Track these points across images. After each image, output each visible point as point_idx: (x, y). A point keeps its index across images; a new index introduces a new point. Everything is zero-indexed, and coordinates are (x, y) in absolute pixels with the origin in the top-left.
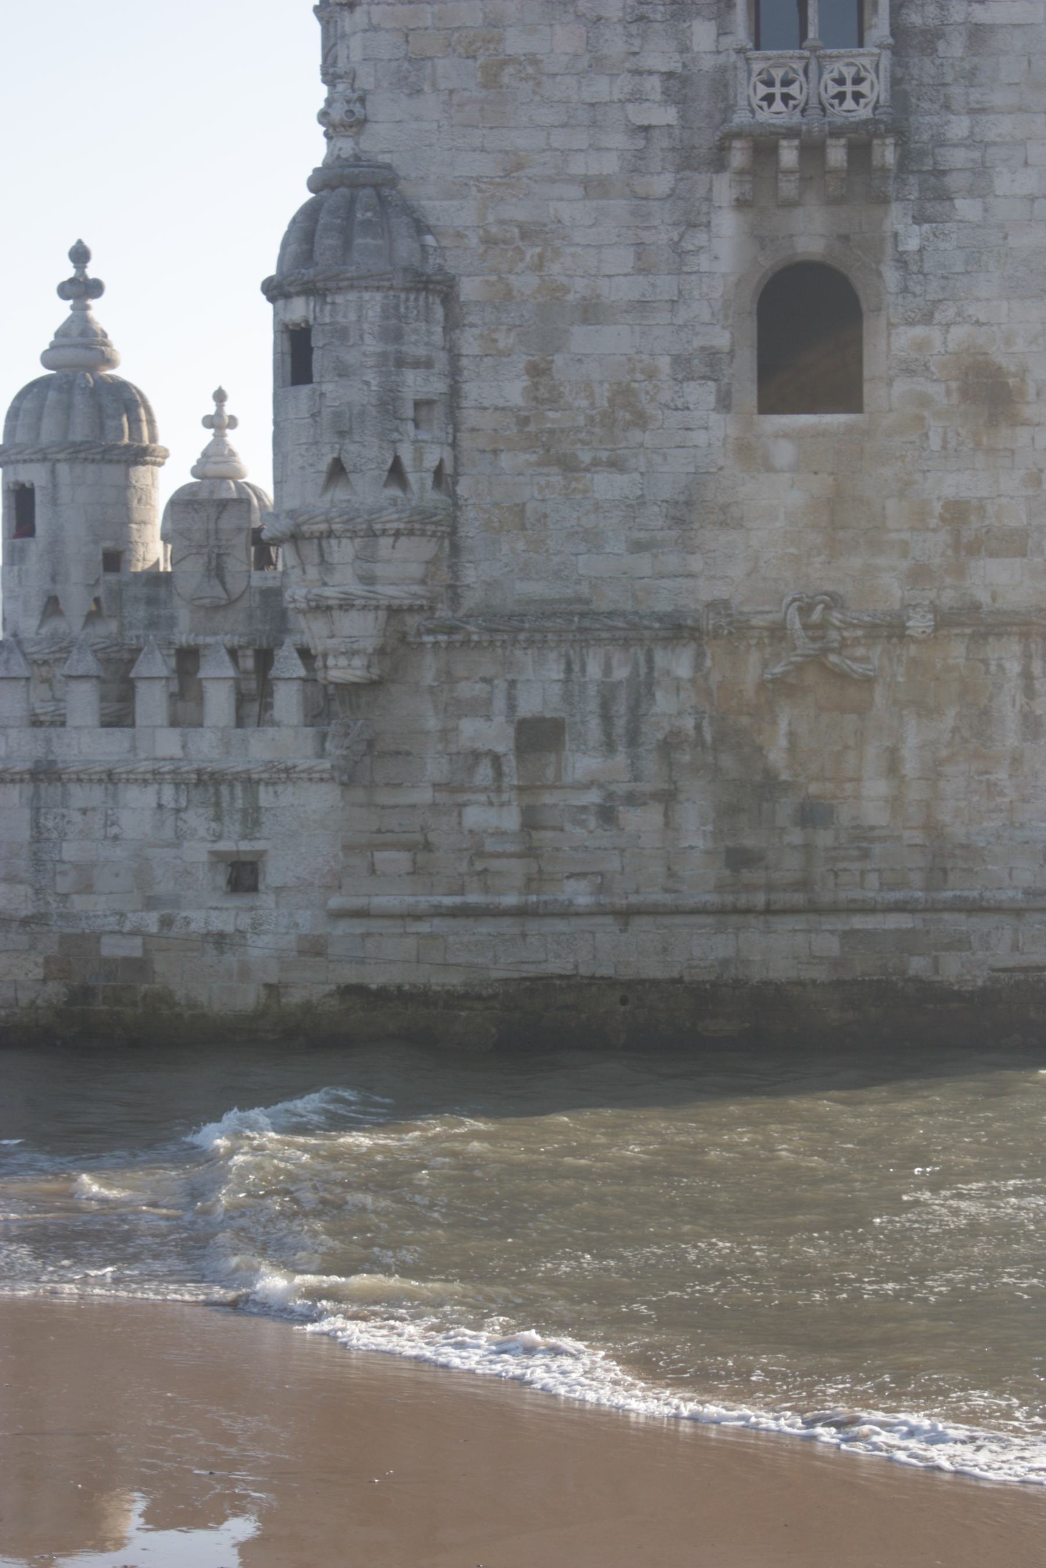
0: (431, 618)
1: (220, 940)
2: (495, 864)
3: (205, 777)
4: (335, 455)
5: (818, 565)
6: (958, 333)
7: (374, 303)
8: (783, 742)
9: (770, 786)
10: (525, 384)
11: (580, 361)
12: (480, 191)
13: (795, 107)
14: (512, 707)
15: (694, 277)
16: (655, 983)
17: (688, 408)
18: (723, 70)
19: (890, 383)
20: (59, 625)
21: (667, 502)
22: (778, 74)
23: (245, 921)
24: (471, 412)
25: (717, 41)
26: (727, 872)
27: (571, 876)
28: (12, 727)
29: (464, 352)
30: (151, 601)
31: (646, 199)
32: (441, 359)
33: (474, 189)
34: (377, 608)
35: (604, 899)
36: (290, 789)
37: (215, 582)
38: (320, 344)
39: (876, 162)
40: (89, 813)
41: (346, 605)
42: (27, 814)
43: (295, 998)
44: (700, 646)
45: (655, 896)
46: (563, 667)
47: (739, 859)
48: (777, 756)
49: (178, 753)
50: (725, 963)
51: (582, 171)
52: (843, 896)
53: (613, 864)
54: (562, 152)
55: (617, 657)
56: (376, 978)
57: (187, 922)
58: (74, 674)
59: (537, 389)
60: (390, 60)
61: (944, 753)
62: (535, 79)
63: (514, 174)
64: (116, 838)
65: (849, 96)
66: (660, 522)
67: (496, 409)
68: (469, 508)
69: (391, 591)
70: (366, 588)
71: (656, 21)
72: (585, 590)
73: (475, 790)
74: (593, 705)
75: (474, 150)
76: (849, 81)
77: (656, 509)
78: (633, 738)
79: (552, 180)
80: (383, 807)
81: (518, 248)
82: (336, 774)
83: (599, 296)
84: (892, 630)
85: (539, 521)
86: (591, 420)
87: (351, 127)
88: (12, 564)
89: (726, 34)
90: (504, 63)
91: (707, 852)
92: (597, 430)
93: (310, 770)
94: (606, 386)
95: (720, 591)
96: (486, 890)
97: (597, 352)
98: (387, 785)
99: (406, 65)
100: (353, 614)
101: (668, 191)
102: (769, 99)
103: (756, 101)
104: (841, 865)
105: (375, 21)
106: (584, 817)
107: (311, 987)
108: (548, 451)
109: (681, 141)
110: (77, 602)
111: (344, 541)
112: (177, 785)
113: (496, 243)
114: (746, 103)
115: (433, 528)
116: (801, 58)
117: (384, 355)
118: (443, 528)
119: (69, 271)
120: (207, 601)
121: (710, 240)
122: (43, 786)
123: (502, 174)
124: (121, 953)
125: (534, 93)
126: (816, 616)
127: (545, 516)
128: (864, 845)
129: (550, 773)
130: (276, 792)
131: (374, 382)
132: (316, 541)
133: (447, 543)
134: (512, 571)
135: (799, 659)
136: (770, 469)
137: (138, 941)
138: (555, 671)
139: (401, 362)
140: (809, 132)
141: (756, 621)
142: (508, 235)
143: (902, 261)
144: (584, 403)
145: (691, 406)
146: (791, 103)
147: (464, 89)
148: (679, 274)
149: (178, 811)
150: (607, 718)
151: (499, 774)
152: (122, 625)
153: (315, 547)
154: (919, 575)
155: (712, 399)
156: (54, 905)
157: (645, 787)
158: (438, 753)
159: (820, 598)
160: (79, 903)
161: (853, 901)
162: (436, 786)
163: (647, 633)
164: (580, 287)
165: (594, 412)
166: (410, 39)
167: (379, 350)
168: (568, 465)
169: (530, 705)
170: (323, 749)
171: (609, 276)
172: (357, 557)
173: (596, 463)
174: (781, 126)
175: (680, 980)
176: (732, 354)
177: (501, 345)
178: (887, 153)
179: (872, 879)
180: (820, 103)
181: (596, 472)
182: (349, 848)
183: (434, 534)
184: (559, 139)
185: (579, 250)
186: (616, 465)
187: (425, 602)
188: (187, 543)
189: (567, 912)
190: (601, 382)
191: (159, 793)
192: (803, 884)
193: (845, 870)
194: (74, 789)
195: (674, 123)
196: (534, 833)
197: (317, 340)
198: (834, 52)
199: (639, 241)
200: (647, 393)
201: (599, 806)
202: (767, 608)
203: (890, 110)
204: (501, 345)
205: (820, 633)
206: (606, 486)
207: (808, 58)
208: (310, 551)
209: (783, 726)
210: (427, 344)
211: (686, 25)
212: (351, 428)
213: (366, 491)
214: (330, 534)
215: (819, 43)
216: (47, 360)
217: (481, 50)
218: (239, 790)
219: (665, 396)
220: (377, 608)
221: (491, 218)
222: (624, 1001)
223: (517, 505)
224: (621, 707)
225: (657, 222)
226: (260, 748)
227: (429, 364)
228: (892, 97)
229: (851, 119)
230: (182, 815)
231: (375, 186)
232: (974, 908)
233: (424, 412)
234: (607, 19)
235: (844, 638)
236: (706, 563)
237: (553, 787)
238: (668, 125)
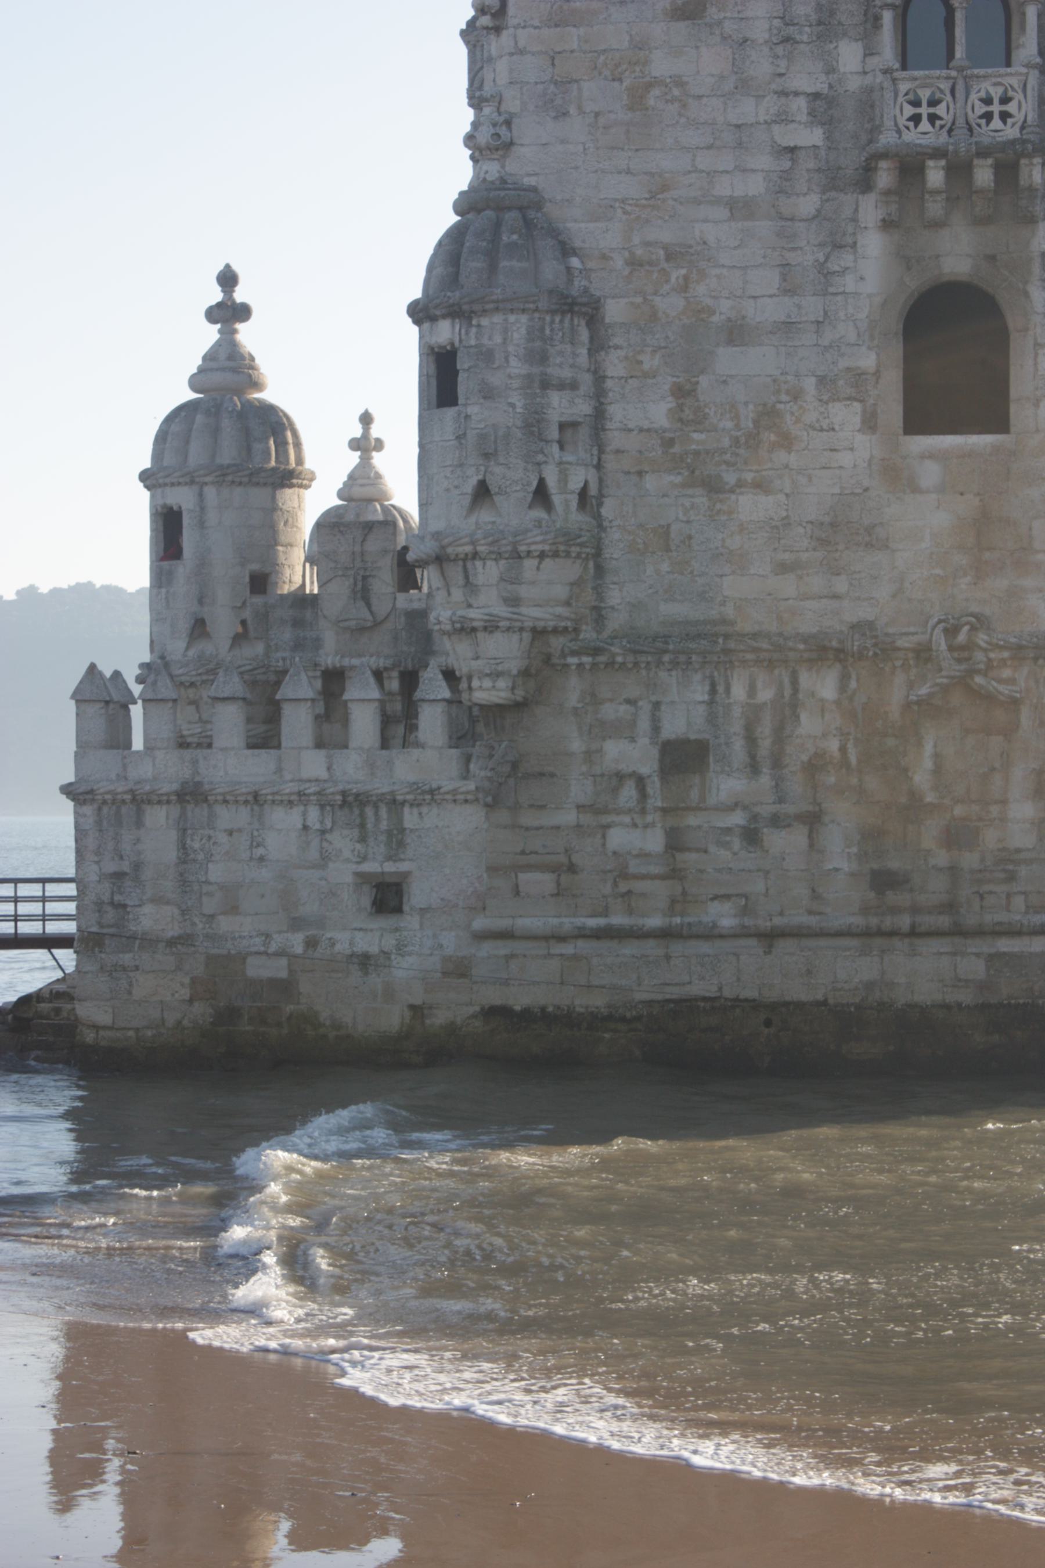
0: (575, 640)
1: (364, 961)
2: (639, 886)
3: (350, 799)
4: (480, 477)
5: (963, 586)
7: (519, 325)
8: (928, 764)
10: (670, 405)
11: (725, 382)
12: (625, 213)
13: (942, 127)
14: (656, 729)
15: (839, 298)
16: (799, 1005)
17: (833, 429)
18: (869, 90)
20: (207, 647)
21: (812, 523)
22: (925, 95)
23: (389, 942)
24: (616, 433)
25: (864, 62)
26: (872, 895)
27: (715, 898)
28: (159, 749)
29: (609, 373)
30: (298, 623)
31: (792, 219)
32: (586, 380)
33: (619, 211)
34: (521, 629)
35: (748, 921)
36: (435, 810)
37: (361, 604)
38: (466, 366)
39: (1023, 182)
41: (491, 627)
42: (173, 835)
43: (439, 1019)
44: (845, 667)
45: (800, 918)
46: (707, 688)
47: (884, 881)
48: (921, 778)
49: (323, 774)
50: (870, 986)
51: (728, 193)
52: (988, 918)
53: (760, 886)
54: (708, 174)
56: (520, 999)
57: (332, 943)
58: (221, 695)
59: (682, 411)
60: (536, 83)
62: (681, 101)
63: (659, 196)
64: (262, 859)
65: (996, 116)
67: (641, 430)
68: (614, 529)
69: (536, 612)
70: (511, 609)
71: (802, 42)
72: (729, 611)
73: (618, 812)
74: (737, 727)
75: (620, 173)
76: (996, 101)
77: (801, 530)
79: (697, 202)
80: (527, 829)
81: (663, 269)
82: (480, 796)
83: (744, 318)
85: (683, 542)
86: (736, 441)
87: (497, 150)
88: (160, 587)
89: (872, 54)
90: (649, 86)
91: (852, 874)
92: (742, 451)
93: (454, 792)
94: (751, 407)
95: (864, 612)
96: (630, 912)
97: (742, 372)
98: (531, 806)
99: (552, 87)
100: (498, 635)
101: (813, 212)
102: (916, 119)
103: (902, 121)
104: (986, 888)
105: (521, 44)
106: (728, 838)
107: (455, 1008)
108: (693, 472)
109: (827, 162)
110: (223, 623)
111: (489, 563)
112: (322, 807)
113: (641, 265)
114: (893, 123)
115: (578, 549)
116: (948, 78)
117: (529, 377)
118: (588, 550)
119: (216, 295)
120: (353, 623)
121: (855, 261)
122: (190, 807)
123: (647, 196)
124: (266, 973)
125: (680, 115)
126: (962, 637)
127: (690, 537)
128: (1011, 867)
129: (694, 794)
130: (420, 814)
131: (519, 404)
132: (461, 563)
133: (591, 564)
134: (657, 592)
135: (945, 681)
136: (916, 489)
137: (284, 962)
138: (699, 693)
139: (546, 384)
140: (956, 152)
141: (900, 643)
142: (654, 257)
144: (729, 425)
145: (837, 427)
146: (938, 123)
147: (610, 112)
148: (824, 295)
149: (323, 832)
150: (751, 740)
151: (643, 795)
153: (460, 569)
155: (857, 420)
157: (790, 809)
158: (583, 774)
159: (965, 619)
160: (225, 924)
161: (1000, 923)
162: (580, 808)
164: (725, 307)
165: (739, 434)
166: (556, 62)
167: (524, 372)
168: (713, 487)
169: (674, 726)
170: (468, 771)
171: (754, 297)
172: (502, 579)
173: (740, 484)
174: (928, 147)
175: (825, 1003)
176: (877, 374)
177: (646, 366)
178: (1034, 173)
179: (1019, 902)
180: (967, 123)
181: (742, 493)
182: (493, 870)
183: (578, 556)
184: (704, 161)
185: (725, 271)
186: (761, 486)
187: (569, 624)
188: (333, 565)
189: (711, 934)
190: (746, 404)
191: (304, 814)
192: (950, 907)
193: (991, 893)
194: (221, 810)
195: (820, 144)
196: (679, 856)
197: (463, 363)
198: (981, 72)
199: (784, 262)
200: (792, 414)
201: (744, 827)
202: (912, 629)
203: (1038, 130)
204: (646, 366)
205: (966, 654)
206: (750, 507)
207: (955, 78)
208: (455, 573)
209: (928, 748)
210: (572, 366)
211: (832, 46)
212: (496, 450)
213: (511, 512)
214: (475, 555)
215: (966, 63)
216: (194, 383)
217: (627, 73)
218: (383, 812)
219: (811, 417)
220: (521, 629)
221: (636, 240)
222: (768, 1023)
223: (663, 527)
224: (765, 731)
226: (405, 769)
227: (574, 386)
228: (1040, 116)
229: (999, 139)
230: (328, 836)
231: (521, 209)
233: (569, 433)
234: (753, 41)
235: (990, 660)
236: (851, 584)
238: (814, 146)
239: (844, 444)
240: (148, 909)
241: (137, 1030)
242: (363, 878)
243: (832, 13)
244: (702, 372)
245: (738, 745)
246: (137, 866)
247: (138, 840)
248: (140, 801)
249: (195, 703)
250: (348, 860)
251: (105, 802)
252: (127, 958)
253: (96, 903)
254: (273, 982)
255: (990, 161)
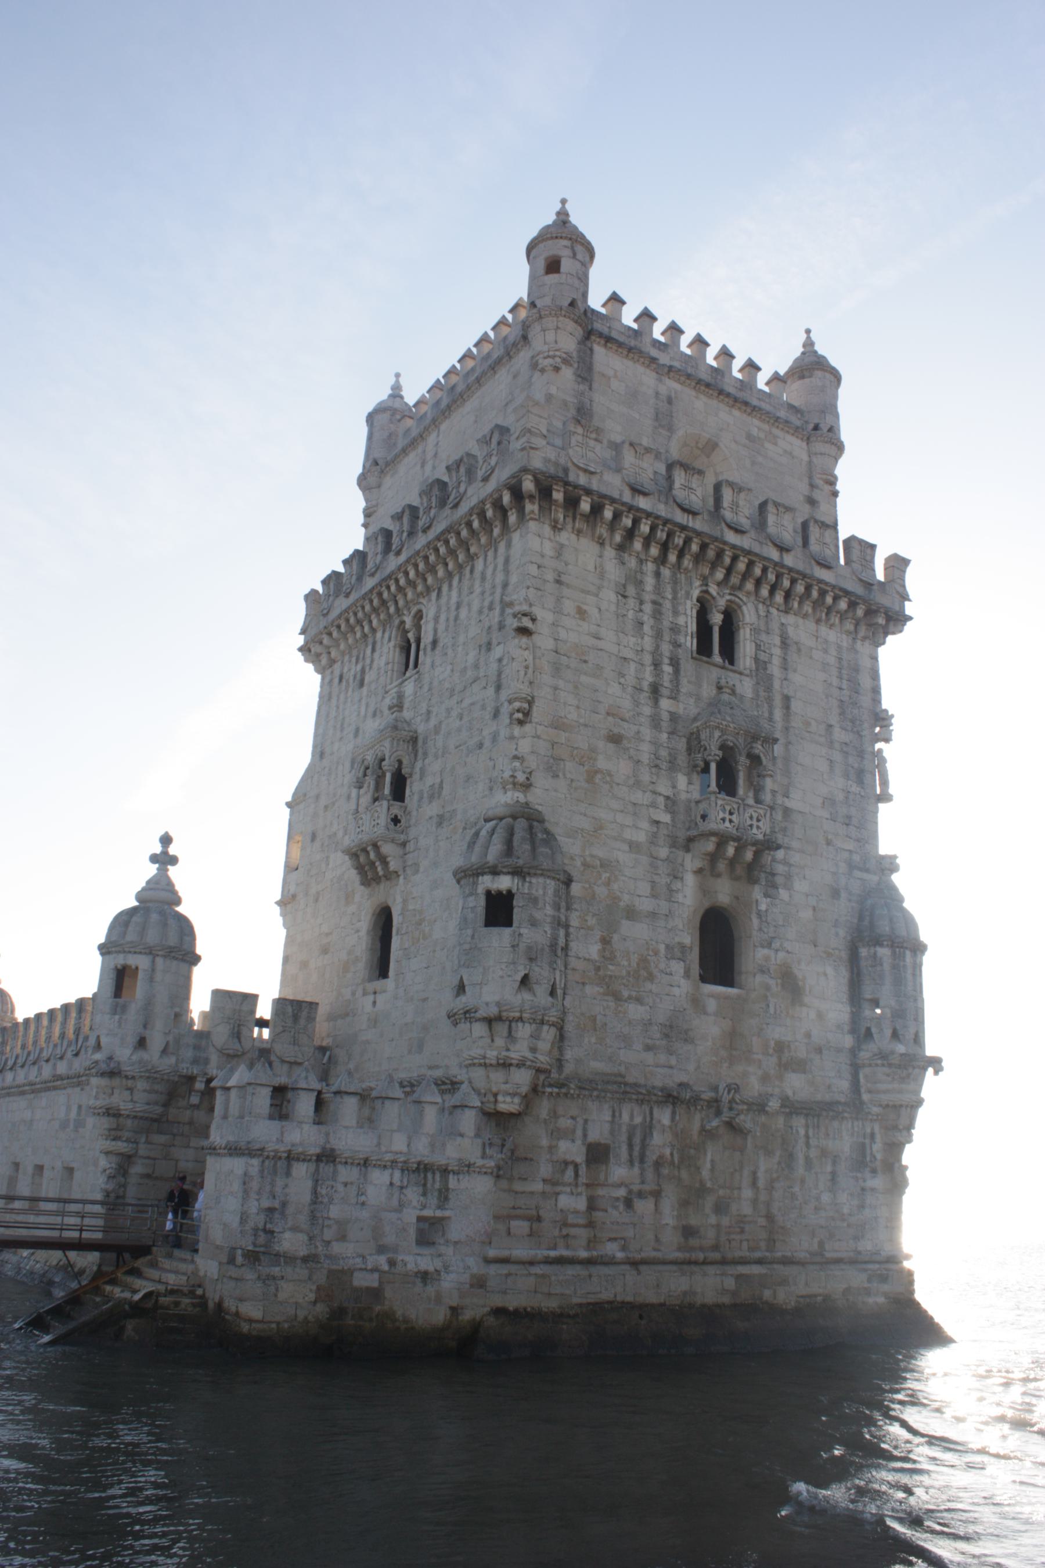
1: (424, 1276)
2: (573, 1231)
6: (781, 955)
7: (551, 884)
8: (708, 1165)
9: (702, 1191)
14: (585, 1135)
19: (754, 976)
20: (145, 1056)
23: (438, 1264)
26: (682, 1240)
27: (610, 1239)
30: (197, 1047)
36: (467, 1177)
37: (236, 1040)
40: (349, 1186)
41: (521, 1064)
42: (309, 1184)
43: (467, 1316)
45: (649, 1253)
46: (611, 1113)
47: (688, 1232)
48: (705, 1173)
49: (405, 1149)
50: (685, 1293)
53: (630, 1233)
55: (637, 1110)
56: (512, 1303)
61: (775, 1175)
64: (363, 1204)
66: (658, 1035)
72: (622, 1069)
73: (564, 1185)
74: (624, 1138)
78: (642, 1159)
80: (516, 1193)
84: (759, 1107)
86: (629, 973)
88: (115, 1013)
90: (596, 772)
91: (674, 1227)
96: (567, 1247)
98: (520, 1178)
99: (552, 761)
100: (523, 1069)
102: (723, 820)
104: (733, 1236)
110: (156, 1042)
111: (527, 1025)
112: (403, 1170)
117: (554, 916)
120: (231, 1052)
122: (322, 1165)
124: (365, 1284)
129: (602, 1177)
136: (705, 1013)
137: (376, 1275)
141: (703, 1096)
143: (759, 915)
144: (626, 963)
149: (402, 1188)
150: (630, 1146)
151: (577, 1175)
152: (177, 1059)
154: (765, 1079)
155: (682, 971)
156: (320, 1248)
157: (647, 1188)
160: (337, 1248)
161: (741, 1257)
163: (654, 1098)
168: (617, 997)
169: (594, 1136)
173: (630, 997)
176: (691, 948)
177: (589, 924)
182: (497, 1218)
184: (620, 818)
186: (639, 1000)
189: (610, 1262)
191: (392, 1175)
192: (716, 1248)
194: (341, 1168)
204: (589, 924)
206: (636, 1012)
208: (501, 1029)
213: (541, 996)
214: (520, 1019)
216: (139, 897)
219: (662, 966)
221: (587, 853)
222: (641, 1317)
224: (637, 1140)
225: (660, 872)
230: (404, 1191)
232: (787, 1261)
237: (604, 1185)
239: (677, 982)
240: (287, 1235)
241: (278, 1323)
242: (420, 1219)
243: (675, 759)
244: (615, 932)
245: (624, 1148)
246: (284, 1204)
247: (286, 1186)
248: (291, 1158)
249: (131, 1089)
250: (415, 1208)
251: (268, 1157)
252: (276, 1271)
253: (253, 1229)
254: (369, 1290)
255: (754, 848)
